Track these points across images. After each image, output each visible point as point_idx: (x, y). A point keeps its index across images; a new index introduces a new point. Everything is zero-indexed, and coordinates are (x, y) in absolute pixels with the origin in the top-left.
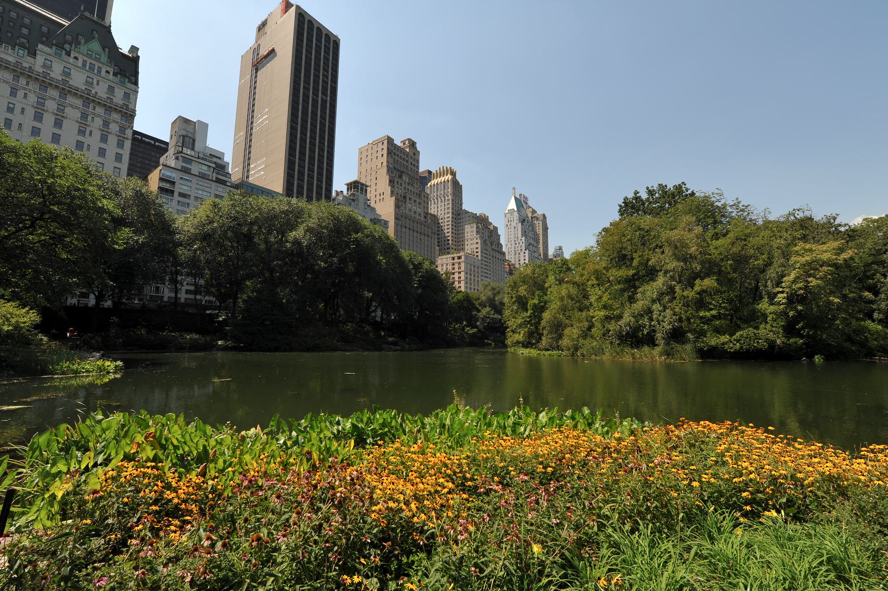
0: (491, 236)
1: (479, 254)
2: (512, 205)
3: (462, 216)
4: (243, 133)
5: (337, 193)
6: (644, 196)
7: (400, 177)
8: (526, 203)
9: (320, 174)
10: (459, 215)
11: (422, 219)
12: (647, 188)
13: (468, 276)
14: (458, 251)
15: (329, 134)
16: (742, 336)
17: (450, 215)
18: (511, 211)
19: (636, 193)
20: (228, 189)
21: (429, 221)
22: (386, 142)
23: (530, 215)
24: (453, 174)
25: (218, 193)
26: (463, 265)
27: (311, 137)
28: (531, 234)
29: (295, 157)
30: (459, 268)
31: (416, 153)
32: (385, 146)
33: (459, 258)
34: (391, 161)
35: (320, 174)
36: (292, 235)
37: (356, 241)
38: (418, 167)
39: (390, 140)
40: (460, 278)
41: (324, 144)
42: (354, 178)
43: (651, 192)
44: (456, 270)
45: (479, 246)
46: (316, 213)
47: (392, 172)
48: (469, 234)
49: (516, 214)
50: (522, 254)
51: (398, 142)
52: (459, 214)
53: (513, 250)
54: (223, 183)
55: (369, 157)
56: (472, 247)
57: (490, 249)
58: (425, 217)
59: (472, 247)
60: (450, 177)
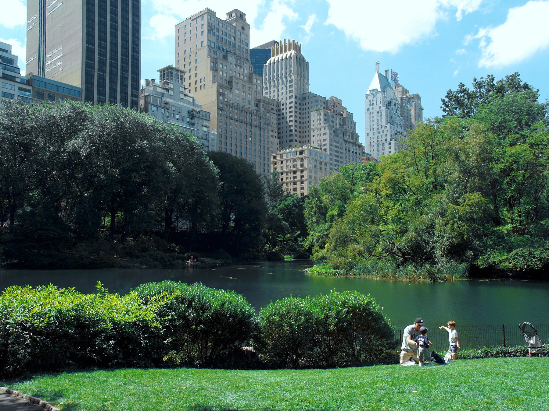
0: (344, 124)
1: (327, 147)
2: (376, 84)
3: (307, 101)
4: (36, 17)
5: (148, 83)
6: (471, 88)
7: (225, 57)
8: (396, 81)
9: (125, 62)
10: (305, 101)
11: (253, 107)
12: (475, 79)
13: (313, 175)
14: (302, 143)
15: (133, 14)
16: (517, 254)
17: (293, 100)
18: (374, 92)
19: (462, 85)
20: (18, 85)
21: (262, 109)
22: (206, 16)
23: (399, 96)
24: (298, 48)
25: (6, 91)
26: (306, 162)
27: (111, 19)
28: (399, 120)
29: (94, 45)
30: (302, 165)
31: (245, 28)
32: (205, 21)
33: (302, 152)
34: (213, 39)
35: (125, 62)
36: (71, 144)
37: (141, 151)
38: (248, 44)
39: (210, 13)
40: (302, 177)
41: (128, 27)
42: (170, 61)
43: (479, 85)
44: (298, 167)
45: (327, 137)
46: (103, 115)
47: (215, 53)
48: (316, 123)
49: (379, 95)
50: (387, 145)
51: (222, 16)
52: (304, 99)
53: (375, 140)
54: (12, 79)
55: (188, 35)
56: (319, 138)
57: (341, 140)
58: (257, 105)
59: (319, 138)
60: (293, 52)
